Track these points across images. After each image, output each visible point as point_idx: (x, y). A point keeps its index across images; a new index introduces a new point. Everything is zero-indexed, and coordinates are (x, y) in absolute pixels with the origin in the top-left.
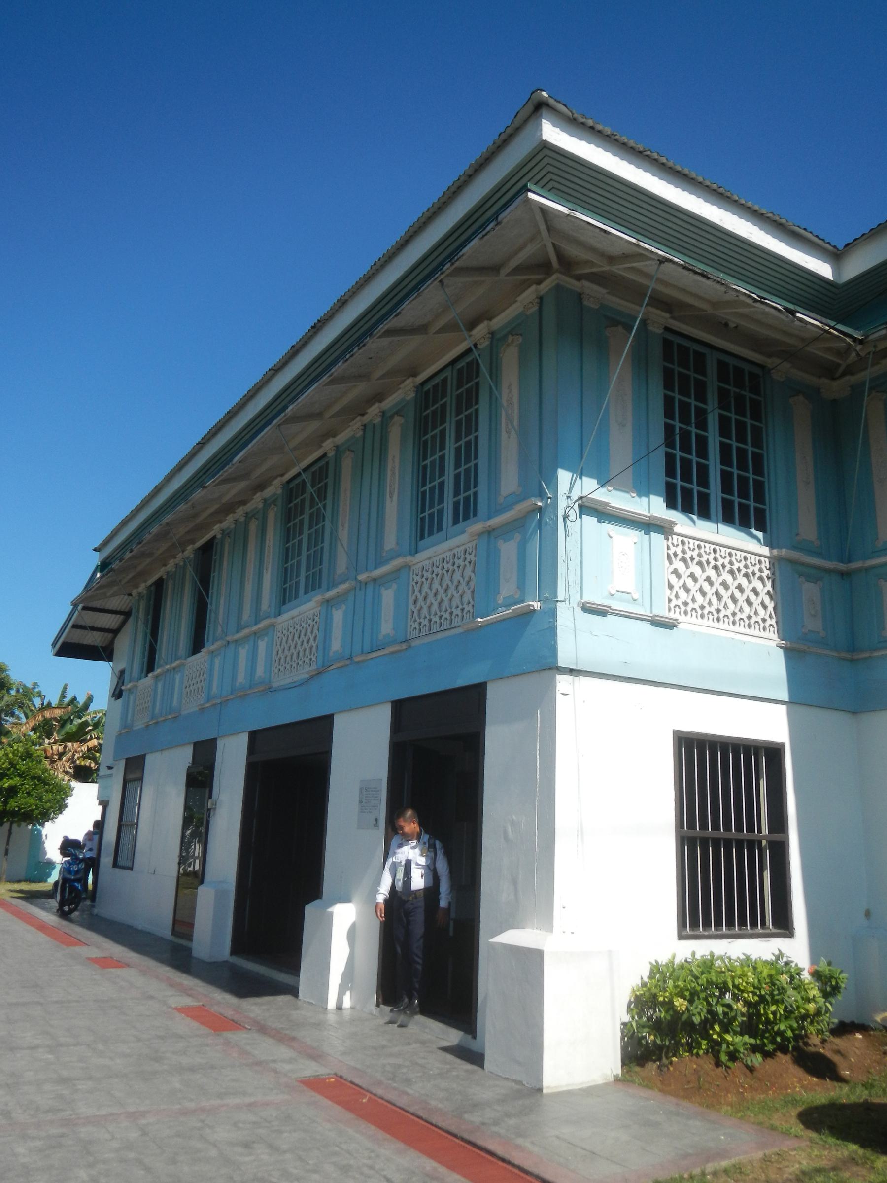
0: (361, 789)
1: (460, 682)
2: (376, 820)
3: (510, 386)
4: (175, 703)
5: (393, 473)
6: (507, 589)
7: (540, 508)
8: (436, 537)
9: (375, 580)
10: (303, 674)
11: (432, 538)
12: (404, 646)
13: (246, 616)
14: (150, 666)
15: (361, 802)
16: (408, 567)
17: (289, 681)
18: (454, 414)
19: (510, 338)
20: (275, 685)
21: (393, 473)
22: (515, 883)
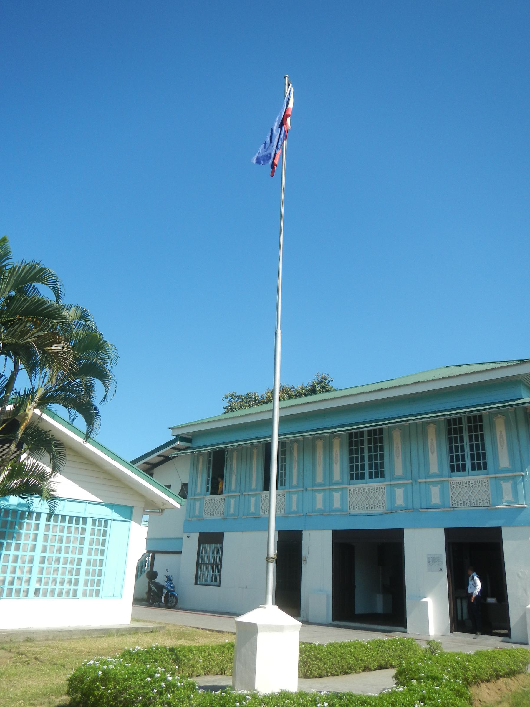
0: (428, 558)
1: (487, 525)
2: (441, 569)
3: (501, 432)
4: (252, 510)
5: (432, 444)
6: (506, 498)
7: (522, 475)
8: (461, 473)
9: (426, 482)
10: (381, 511)
11: (459, 473)
12: (452, 509)
13: (319, 479)
14: (215, 488)
15: (429, 562)
16: (448, 481)
17: (366, 512)
18: (467, 431)
19: (499, 416)
20: (353, 512)
21: (432, 444)
22: (525, 590)
